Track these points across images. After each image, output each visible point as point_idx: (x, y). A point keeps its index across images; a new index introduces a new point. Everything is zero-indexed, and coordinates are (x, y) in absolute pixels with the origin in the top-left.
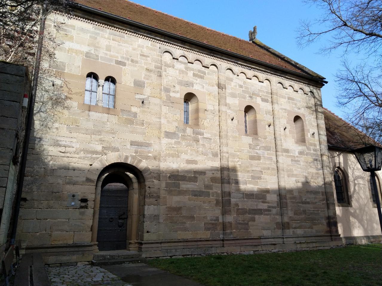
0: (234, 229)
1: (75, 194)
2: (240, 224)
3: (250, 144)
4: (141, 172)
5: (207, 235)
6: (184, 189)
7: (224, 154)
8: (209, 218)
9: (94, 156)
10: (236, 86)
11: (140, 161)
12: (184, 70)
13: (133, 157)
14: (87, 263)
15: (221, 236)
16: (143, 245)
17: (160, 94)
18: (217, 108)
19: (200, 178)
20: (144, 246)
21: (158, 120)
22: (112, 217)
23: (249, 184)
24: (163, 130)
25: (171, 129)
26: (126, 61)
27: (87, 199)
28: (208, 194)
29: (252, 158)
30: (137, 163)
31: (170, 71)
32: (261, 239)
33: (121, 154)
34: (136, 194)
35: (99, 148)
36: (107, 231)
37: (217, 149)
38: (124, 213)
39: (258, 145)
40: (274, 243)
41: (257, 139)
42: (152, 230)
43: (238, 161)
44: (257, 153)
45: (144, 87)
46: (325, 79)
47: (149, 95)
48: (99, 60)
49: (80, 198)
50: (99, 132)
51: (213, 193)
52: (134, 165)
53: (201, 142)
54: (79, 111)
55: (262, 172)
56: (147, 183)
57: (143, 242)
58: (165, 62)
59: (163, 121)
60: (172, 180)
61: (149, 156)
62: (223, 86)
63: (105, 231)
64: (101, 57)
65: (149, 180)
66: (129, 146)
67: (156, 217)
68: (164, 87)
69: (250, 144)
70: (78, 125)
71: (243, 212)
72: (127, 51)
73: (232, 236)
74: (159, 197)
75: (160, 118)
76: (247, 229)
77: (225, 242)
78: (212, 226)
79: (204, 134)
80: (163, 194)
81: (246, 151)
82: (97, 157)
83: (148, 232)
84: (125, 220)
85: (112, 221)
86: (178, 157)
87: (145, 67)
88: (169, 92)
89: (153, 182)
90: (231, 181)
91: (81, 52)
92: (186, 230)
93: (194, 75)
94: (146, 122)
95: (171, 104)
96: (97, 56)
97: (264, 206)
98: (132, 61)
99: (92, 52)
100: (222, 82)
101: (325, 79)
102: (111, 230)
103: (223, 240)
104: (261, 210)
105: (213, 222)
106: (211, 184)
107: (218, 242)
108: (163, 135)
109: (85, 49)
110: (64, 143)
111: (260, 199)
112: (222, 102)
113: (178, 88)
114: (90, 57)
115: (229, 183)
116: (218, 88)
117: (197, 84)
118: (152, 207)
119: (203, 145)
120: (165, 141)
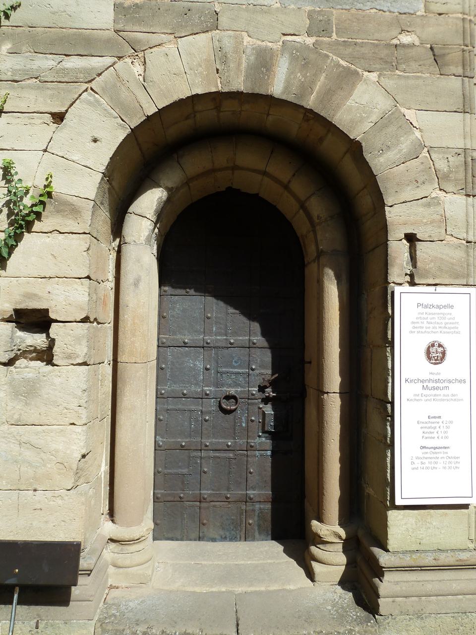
4: (355, 149)
9: (73, 63)
11: (347, 79)
13: (303, 60)
22: (232, 391)
27: (47, 311)
30: (328, 95)
33: (228, 44)
36: (212, 454)
52: (311, 102)
56: (399, 216)
61: (404, 46)
63: (204, 454)
82: (85, 71)
89: (437, 202)
102: (228, 449)
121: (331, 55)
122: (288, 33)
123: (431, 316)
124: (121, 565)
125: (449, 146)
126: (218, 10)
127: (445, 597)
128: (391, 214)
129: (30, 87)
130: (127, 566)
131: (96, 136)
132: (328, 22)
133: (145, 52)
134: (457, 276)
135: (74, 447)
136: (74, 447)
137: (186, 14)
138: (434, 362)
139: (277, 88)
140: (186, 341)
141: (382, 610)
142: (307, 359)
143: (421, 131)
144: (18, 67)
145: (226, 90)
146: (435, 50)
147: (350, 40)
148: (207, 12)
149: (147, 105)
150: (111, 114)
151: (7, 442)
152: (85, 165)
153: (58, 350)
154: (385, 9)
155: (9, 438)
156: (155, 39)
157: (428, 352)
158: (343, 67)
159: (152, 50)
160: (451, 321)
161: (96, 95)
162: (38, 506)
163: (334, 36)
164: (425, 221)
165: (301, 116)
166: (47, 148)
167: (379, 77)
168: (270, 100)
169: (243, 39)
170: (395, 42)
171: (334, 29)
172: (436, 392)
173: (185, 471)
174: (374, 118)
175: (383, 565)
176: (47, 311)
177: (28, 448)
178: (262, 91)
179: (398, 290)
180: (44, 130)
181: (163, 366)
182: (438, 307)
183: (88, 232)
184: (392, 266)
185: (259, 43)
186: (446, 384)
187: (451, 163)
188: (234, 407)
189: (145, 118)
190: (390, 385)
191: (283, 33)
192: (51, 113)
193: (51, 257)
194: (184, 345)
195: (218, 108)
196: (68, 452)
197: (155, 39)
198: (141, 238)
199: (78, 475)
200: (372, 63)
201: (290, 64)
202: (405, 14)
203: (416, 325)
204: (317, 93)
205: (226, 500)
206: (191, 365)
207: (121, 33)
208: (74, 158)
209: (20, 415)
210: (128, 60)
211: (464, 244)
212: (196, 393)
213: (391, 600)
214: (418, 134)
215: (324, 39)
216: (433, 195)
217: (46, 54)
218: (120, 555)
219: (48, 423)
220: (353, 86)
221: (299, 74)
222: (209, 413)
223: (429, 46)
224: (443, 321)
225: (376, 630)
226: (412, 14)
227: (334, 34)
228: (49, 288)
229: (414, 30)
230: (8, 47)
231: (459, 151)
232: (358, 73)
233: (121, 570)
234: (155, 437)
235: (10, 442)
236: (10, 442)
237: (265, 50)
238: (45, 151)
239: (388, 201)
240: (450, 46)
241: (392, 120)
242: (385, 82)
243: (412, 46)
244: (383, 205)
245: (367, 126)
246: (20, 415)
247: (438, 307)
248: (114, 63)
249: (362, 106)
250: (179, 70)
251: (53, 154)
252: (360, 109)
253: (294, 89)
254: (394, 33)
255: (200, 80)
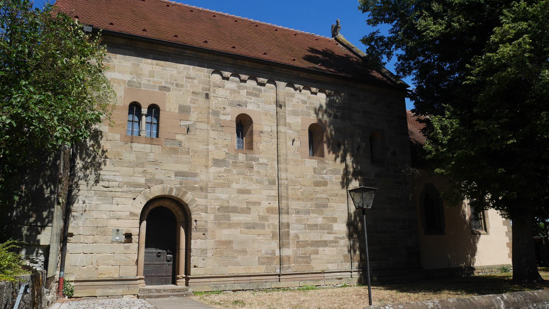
0: (293, 263)
1: (119, 228)
2: (300, 257)
3: (314, 169)
4: (187, 205)
5: (262, 270)
6: (236, 222)
7: (283, 181)
8: (263, 252)
9: (137, 189)
10: (298, 102)
11: (185, 193)
12: (236, 89)
13: (178, 189)
14: (133, 296)
15: (278, 271)
17: (208, 118)
18: (275, 129)
19: (253, 208)
20: (190, 281)
21: (205, 147)
23: (312, 213)
24: (211, 157)
25: (220, 155)
26: (170, 86)
28: (263, 227)
29: (317, 184)
30: (182, 195)
31: (220, 92)
32: (325, 273)
33: (165, 186)
35: (142, 180)
37: (275, 175)
39: (325, 169)
40: (340, 277)
41: (323, 162)
42: (199, 265)
43: (300, 189)
44: (323, 178)
45: (190, 112)
46: (409, 87)
47: (195, 120)
48: (142, 88)
49: (124, 233)
50: (142, 165)
51: (269, 225)
52: (179, 197)
53: (255, 169)
54: (122, 143)
55: (328, 199)
56: (194, 217)
57: (189, 276)
58: (214, 83)
59: (211, 147)
60: (222, 212)
62: (282, 104)
64: (144, 84)
65: (196, 213)
66: (173, 177)
67: (204, 251)
68: (213, 110)
69: (314, 169)
70: (121, 158)
71: (306, 244)
72: (172, 76)
73: (290, 270)
74: (206, 230)
75: (207, 145)
76: (309, 263)
77: (281, 277)
78: (267, 260)
79: (260, 159)
80: (210, 226)
81: (310, 176)
83: (195, 267)
86: (229, 186)
87: (192, 90)
88: (218, 115)
89: (200, 214)
90: (290, 210)
91: (124, 82)
92: (237, 264)
93: (248, 93)
94: (192, 150)
95: (220, 129)
96: (140, 84)
97: (331, 237)
98: (177, 85)
99: (135, 80)
100: (281, 99)
101: (409, 87)
103: (279, 275)
104: (325, 242)
105: (269, 256)
106: (267, 215)
107: (274, 277)
108: (210, 163)
109: (127, 78)
110: (107, 177)
111: (326, 230)
112: (282, 121)
113: (229, 109)
114: (132, 86)
115: (288, 213)
116: (277, 106)
117: (251, 103)
118: (199, 241)
119: (258, 172)
120: (213, 170)
128: (192, 216)
139: (173, 194)
241: (193, 200)
250: (156, 191)
252: (187, 198)
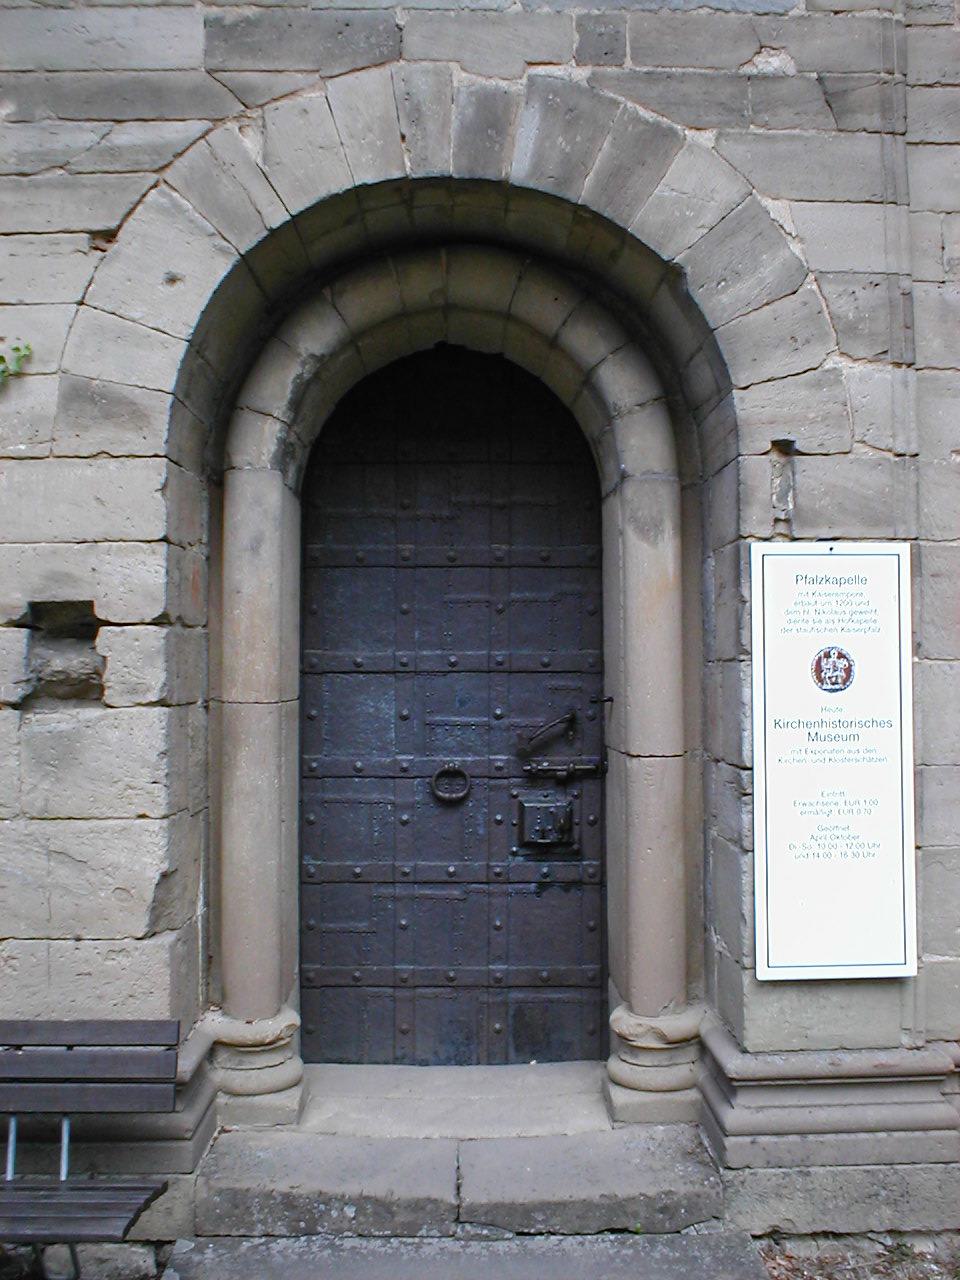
4: (673, 274)
9: (130, 135)
11: (657, 143)
13: (567, 109)
16: (742, 1099)
22: (456, 761)
27: (90, 604)
30: (617, 176)
33: (423, 85)
34: (649, 530)
38: (572, 722)
52: (584, 191)
56: (760, 406)
61: (764, 77)
63: (399, 890)
82: (155, 149)
84: (589, 786)
85: (460, 801)
102: (451, 881)
121: (621, 99)
122: (539, 60)
123: (824, 599)
124: (241, 1091)
125: (856, 270)
126: (401, 23)
127: (853, 1136)
129: (50, 184)
130: (251, 1091)
131: (175, 271)
132: (617, 36)
133: (266, 107)
134: (876, 522)
135: (147, 860)
136: (147, 860)
137: (340, 33)
138: (830, 687)
139: (518, 167)
140: (359, 660)
141: (732, 1159)
142: (608, 694)
143: (802, 241)
144: (28, 148)
145: (420, 174)
146: (826, 83)
147: (660, 69)
148: (381, 28)
149: (270, 209)
150: (202, 229)
151: (24, 851)
152: (155, 326)
153: (113, 678)
154: (728, 8)
155: (27, 843)
156: (283, 83)
157: (818, 669)
158: (647, 122)
159: (278, 104)
160: (863, 608)
161: (175, 194)
162: (86, 969)
163: (628, 63)
164: (812, 415)
165: (569, 216)
166: (83, 298)
167: (717, 139)
168: (504, 189)
169: (451, 75)
170: (748, 70)
171: (628, 49)
172: (834, 745)
173: (363, 925)
174: (709, 218)
175: (734, 1076)
176: (90, 604)
177: (62, 862)
178: (490, 174)
179: (757, 549)
180: (76, 266)
181: (314, 712)
182: (839, 582)
183: (162, 454)
184: (748, 503)
185: (482, 81)
186: (854, 730)
187: (860, 302)
188: (461, 794)
189: (265, 233)
190: (746, 734)
191: (529, 60)
192: (90, 232)
193: (94, 503)
194: (354, 668)
195: (408, 203)
196: (137, 868)
197: (283, 83)
198: (263, 458)
199: (157, 912)
200: (702, 113)
201: (543, 119)
202: (766, 14)
203: (793, 617)
204: (597, 174)
205: (447, 983)
206: (371, 710)
207: (216, 75)
208: (136, 315)
209: (47, 800)
210: (233, 126)
211: (889, 460)
212: (383, 766)
213: (748, 1139)
214: (796, 248)
215: (609, 69)
216: (828, 365)
217: (80, 120)
218: (237, 1072)
219: (98, 815)
220: (666, 158)
221: (561, 139)
222: (411, 807)
223: (815, 75)
224: (848, 609)
225: (718, 1193)
226: (781, 15)
227: (628, 58)
228: (93, 561)
229: (784, 45)
230: (8, 111)
231: (876, 279)
232: (674, 133)
233: (241, 1100)
234: (301, 858)
235: (29, 850)
236: (29, 850)
237: (495, 95)
238: (81, 303)
239: (740, 378)
240: (856, 75)
241: (743, 224)
242: (731, 148)
243: (782, 77)
244: (730, 387)
245: (694, 234)
246: (47, 800)
247: (839, 582)
248: (207, 133)
249: (684, 196)
250: (330, 139)
251: (95, 308)
252: (678, 204)
253: (552, 168)
254: (746, 52)
255: (370, 156)
